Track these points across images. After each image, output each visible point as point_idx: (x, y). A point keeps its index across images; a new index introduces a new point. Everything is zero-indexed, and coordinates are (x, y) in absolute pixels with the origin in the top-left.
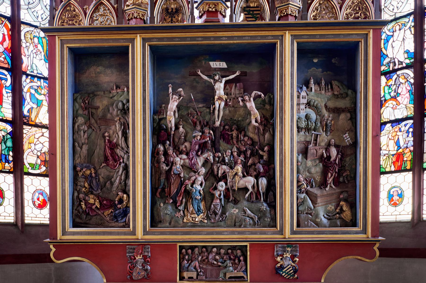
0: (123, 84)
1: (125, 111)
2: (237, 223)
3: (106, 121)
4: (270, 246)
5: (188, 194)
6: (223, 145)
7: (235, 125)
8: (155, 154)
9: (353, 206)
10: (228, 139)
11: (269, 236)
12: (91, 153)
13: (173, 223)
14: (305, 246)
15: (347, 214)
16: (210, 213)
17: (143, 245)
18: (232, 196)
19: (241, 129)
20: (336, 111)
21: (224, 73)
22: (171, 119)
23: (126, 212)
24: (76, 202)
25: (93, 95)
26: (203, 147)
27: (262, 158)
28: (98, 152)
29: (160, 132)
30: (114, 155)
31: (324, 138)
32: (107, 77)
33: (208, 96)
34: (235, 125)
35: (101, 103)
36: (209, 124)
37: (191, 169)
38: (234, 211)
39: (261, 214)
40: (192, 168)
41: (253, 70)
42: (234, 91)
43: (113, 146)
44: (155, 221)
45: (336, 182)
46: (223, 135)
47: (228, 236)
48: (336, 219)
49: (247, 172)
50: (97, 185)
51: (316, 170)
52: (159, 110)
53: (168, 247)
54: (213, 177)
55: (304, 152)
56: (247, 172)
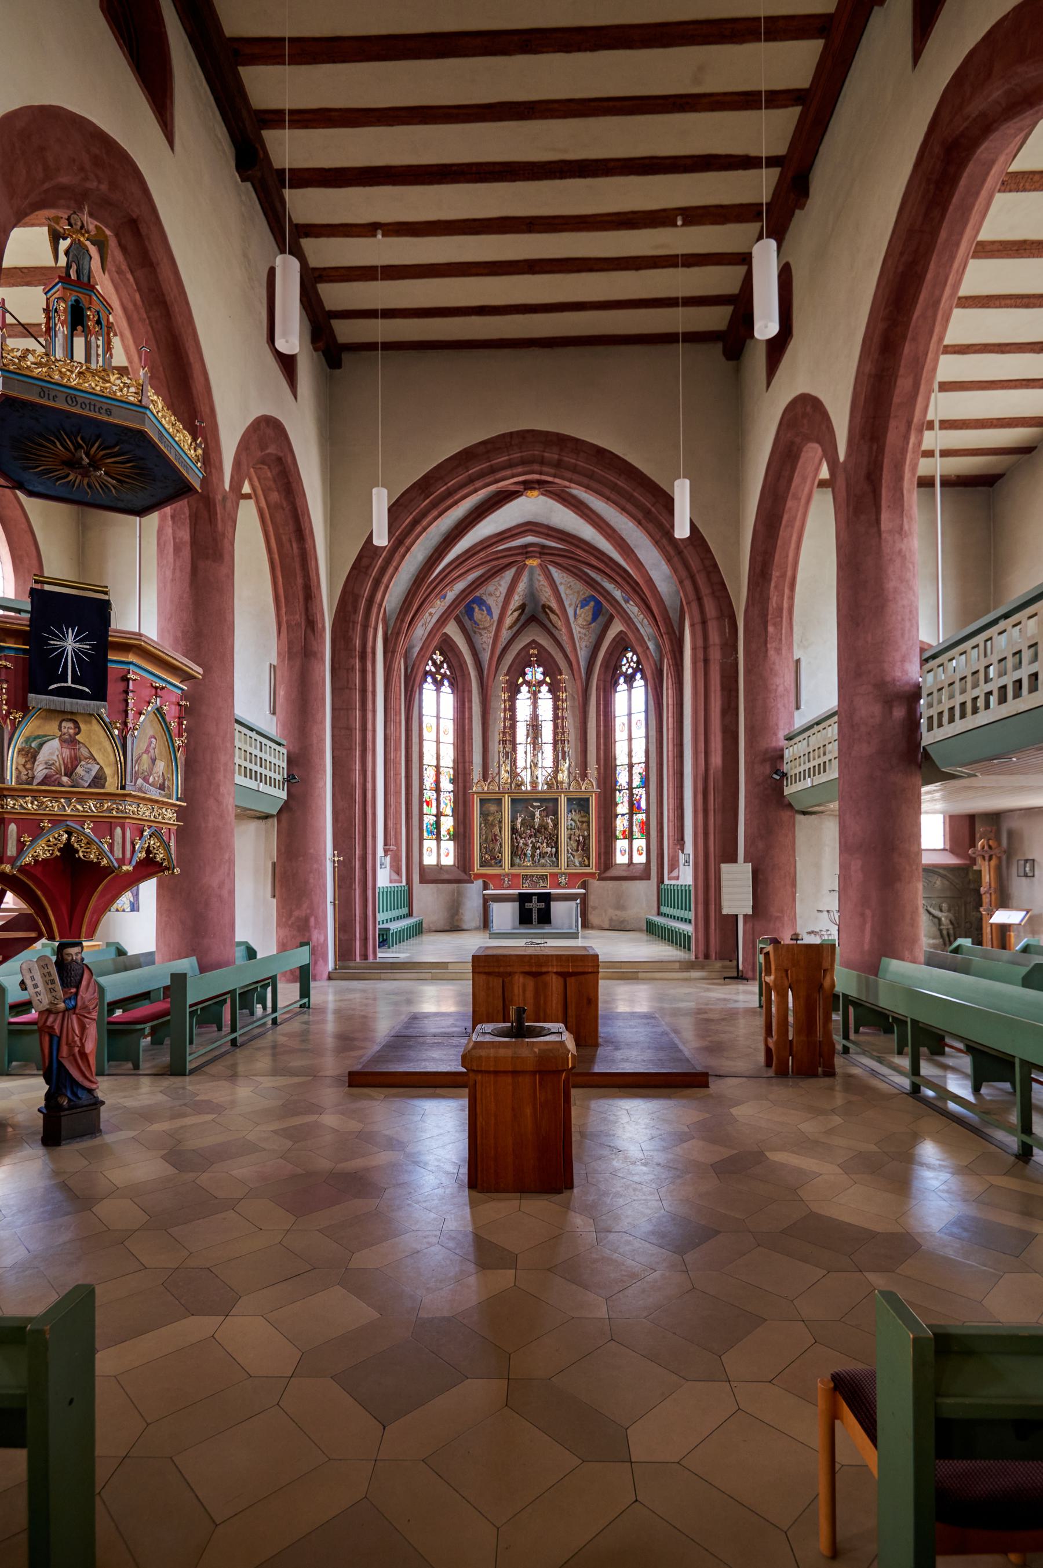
0: (500, 811)
1: (500, 822)
2: (543, 866)
3: (493, 825)
4: (557, 875)
5: (525, 854)
6: (538, 835)
7: (544, 827)
8: (512, 838)
9: (589, 859)
10: (540, 832)
11: (555, 870)
12: (486, 838)
13: (519, 866)
14: (570, 875)
15: (586, 862)
16: (534, 862)
17: (507, 874)
18: (542, 855)
19: (546, 829)
20: (582, 822)
21: (539, 807)
22: (519, 826)
23: (501, 861)
24: (481, 857)
25: (488, 815)
26: (531, 836)
27: (553, 840)
28: (490, 837)
29: (514, 830)
30: (495, 839)
31: (577, 832)
32: (493, 808)
33: (533, 816)
34: (544, 827)
35: (491, 818)
36: (533, 827)
37: (526, 845)
38: (542, 861)
39: (553, 862)
40: (527, 844)
41: (551, 805)
42: (543, 814)
43: (495, 835)
44: (512, 865)
45: (583, 850)
46: (539, 831)
47: (541, 871)
48: (582, 864)
49: (548, 846)
50: (490, 851)
51: (575, 845)
52: (513, 821)
53: (518, 875)
54: (534, 848)
55: (570, 838)
56: (548, 846)
